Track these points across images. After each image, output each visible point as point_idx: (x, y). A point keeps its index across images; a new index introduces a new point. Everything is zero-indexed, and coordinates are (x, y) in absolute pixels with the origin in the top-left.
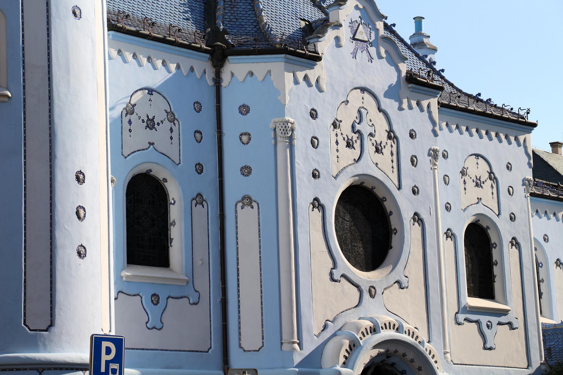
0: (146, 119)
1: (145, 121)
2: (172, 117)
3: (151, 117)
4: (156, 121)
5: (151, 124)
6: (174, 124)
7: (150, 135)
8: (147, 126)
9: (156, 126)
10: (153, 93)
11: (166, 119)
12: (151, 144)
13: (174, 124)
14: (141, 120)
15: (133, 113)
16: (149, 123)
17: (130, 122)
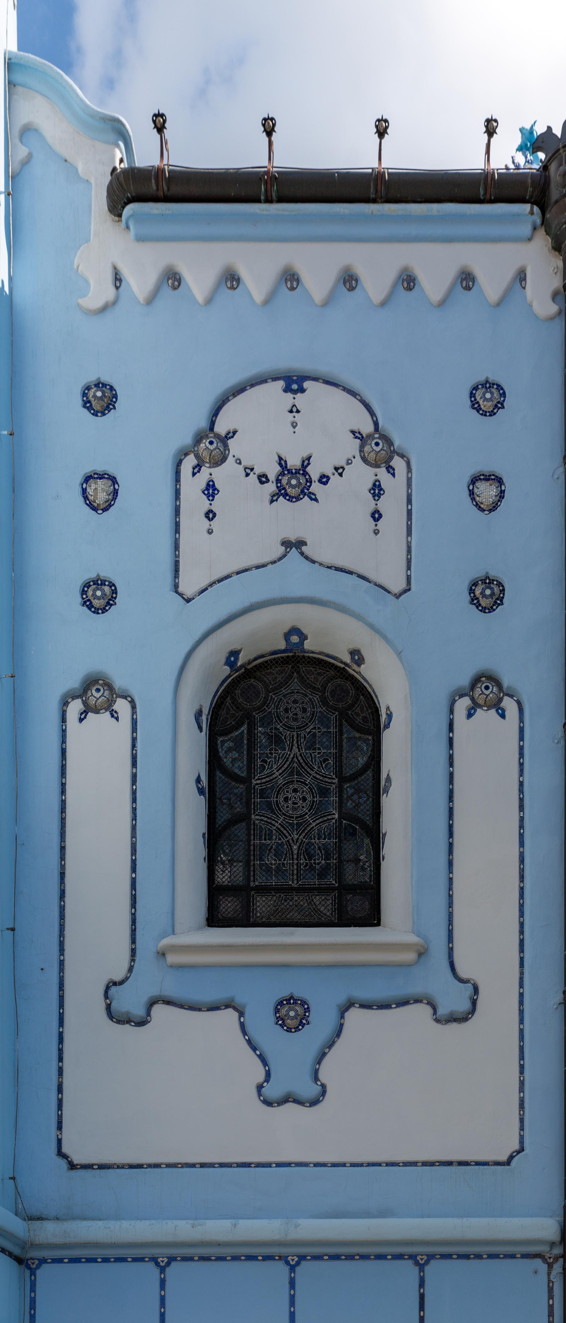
0: (273, 471)
1: (272, 477)
2: (379, 448)
3: (294, 462)
4: (314, 471)
5: (294, 482)
6: (391, 470)
7: (293, 518)
8: (281, 493)
9: (316, 487)
10: (306, 384)
11: (358, 461)
12: (294, 545)
13: (391, 470)
14: (253, 478)
15: (224, 459)
16: (285, 480)
17: (211, 490)
